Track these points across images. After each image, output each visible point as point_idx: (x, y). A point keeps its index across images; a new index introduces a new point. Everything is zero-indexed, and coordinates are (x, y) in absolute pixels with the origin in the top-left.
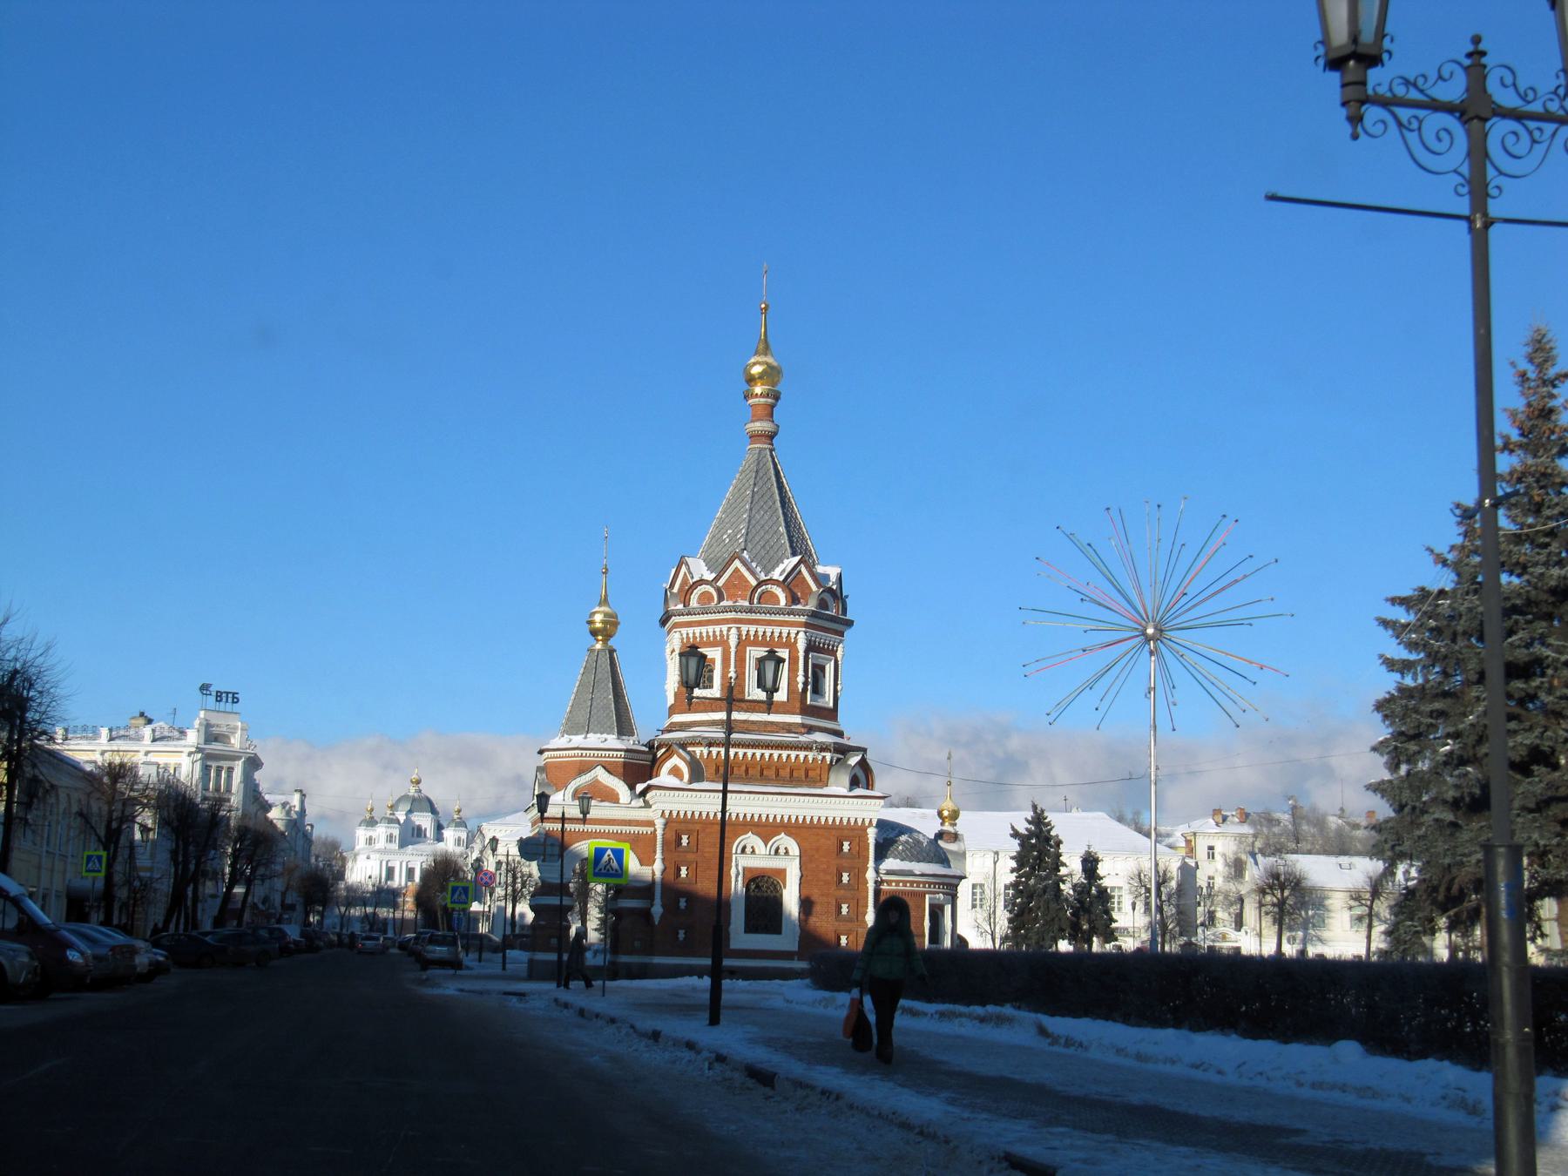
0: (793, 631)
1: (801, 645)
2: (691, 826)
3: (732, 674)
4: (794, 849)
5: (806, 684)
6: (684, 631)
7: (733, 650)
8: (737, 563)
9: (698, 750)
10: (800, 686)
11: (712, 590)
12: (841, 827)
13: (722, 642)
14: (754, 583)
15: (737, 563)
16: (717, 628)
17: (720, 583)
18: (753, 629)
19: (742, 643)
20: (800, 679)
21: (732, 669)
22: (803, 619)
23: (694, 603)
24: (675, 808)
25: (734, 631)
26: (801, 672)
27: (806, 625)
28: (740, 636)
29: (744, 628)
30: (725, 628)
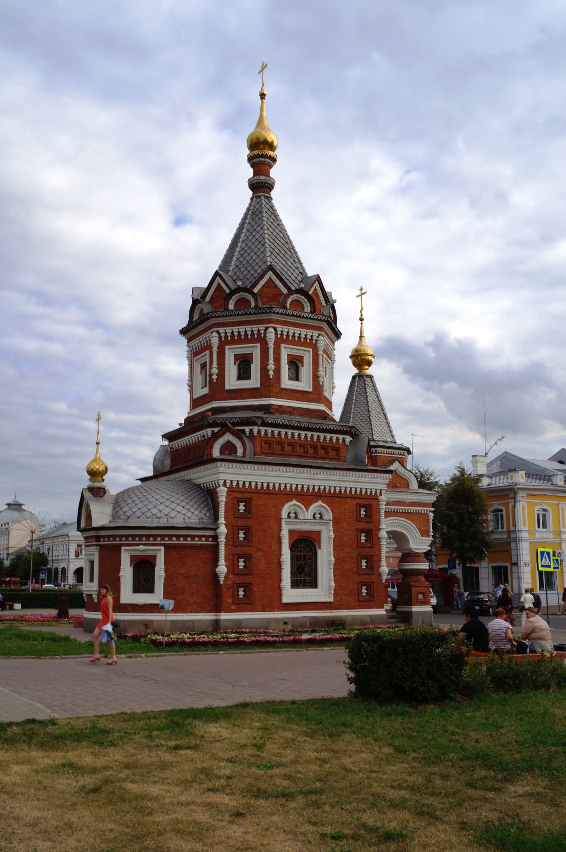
0: (315, 333)
2: (247, 495)
4: (329, 515)
6: (222, 330)
7: (271, 345)
8: (270, 274)
9: (247, 429)
12: (361, 497)
13: (262, 340)
15: (270, 274)
16: (255, 328)
17: (256, 290)
18: (286, 329)
21: (271, 361)
23: (231, 306)
24: (235, 478)
25: (272, 330)
28: (276, 334)
29: (280, 328)
30: (262, 327)
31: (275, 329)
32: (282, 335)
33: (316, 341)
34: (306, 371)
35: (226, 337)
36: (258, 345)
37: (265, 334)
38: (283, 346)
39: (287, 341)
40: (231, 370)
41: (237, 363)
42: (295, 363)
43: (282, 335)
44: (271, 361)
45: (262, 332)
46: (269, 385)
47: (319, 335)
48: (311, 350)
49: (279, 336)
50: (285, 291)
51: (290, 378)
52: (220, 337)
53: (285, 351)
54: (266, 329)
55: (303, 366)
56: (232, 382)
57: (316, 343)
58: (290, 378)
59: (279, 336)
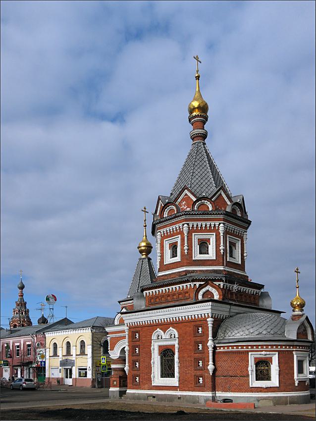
0: (217, 223)
1: (222, 229)
3: (186, 248)
5: (225, 250)
10: (222, 251)
11: (174, 208)
14: (194, 199)
17: (177, 203)
19: (190, 233)
20: (222, 248)
21: (186, 244)
22: (222, 217)
23: (165, 215)
26: (222, 244)
27: (224, 220)
28: (189, 228)
30: (181, 225)
31: (188, 224)
32: (193, 227)
33: (218, 227)
34: (212, 248)
35: (164, 234)
36: (179, 236)
37: (183, 228)
38: (193, 234)
39: (197, 231)
40: (168, 252)
41: (171, 249)
42: (203, 246)
43: (193, 227)
44: (186, 244)
45: (181, 227)
46: (187, 259)
47: (219, 225)
48: (215, 234)
49: (191, 228)
50: (194, 199)
51: (200, 253)
52: (161, 235)
53: (196, 237)
54: (183, 225)
55: (210, 244)
56: (168, 260)
57: (218, 229)
58: (200, 253)
59: (191, 228)
